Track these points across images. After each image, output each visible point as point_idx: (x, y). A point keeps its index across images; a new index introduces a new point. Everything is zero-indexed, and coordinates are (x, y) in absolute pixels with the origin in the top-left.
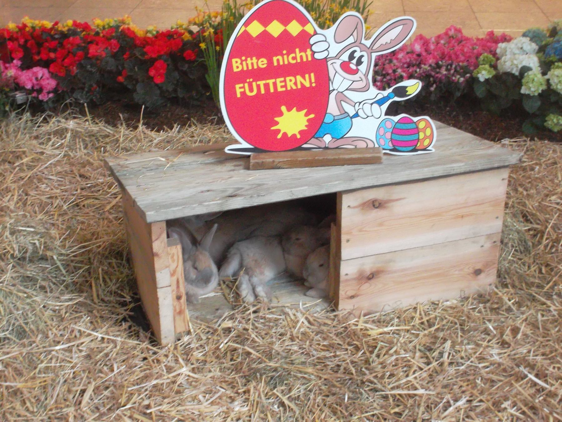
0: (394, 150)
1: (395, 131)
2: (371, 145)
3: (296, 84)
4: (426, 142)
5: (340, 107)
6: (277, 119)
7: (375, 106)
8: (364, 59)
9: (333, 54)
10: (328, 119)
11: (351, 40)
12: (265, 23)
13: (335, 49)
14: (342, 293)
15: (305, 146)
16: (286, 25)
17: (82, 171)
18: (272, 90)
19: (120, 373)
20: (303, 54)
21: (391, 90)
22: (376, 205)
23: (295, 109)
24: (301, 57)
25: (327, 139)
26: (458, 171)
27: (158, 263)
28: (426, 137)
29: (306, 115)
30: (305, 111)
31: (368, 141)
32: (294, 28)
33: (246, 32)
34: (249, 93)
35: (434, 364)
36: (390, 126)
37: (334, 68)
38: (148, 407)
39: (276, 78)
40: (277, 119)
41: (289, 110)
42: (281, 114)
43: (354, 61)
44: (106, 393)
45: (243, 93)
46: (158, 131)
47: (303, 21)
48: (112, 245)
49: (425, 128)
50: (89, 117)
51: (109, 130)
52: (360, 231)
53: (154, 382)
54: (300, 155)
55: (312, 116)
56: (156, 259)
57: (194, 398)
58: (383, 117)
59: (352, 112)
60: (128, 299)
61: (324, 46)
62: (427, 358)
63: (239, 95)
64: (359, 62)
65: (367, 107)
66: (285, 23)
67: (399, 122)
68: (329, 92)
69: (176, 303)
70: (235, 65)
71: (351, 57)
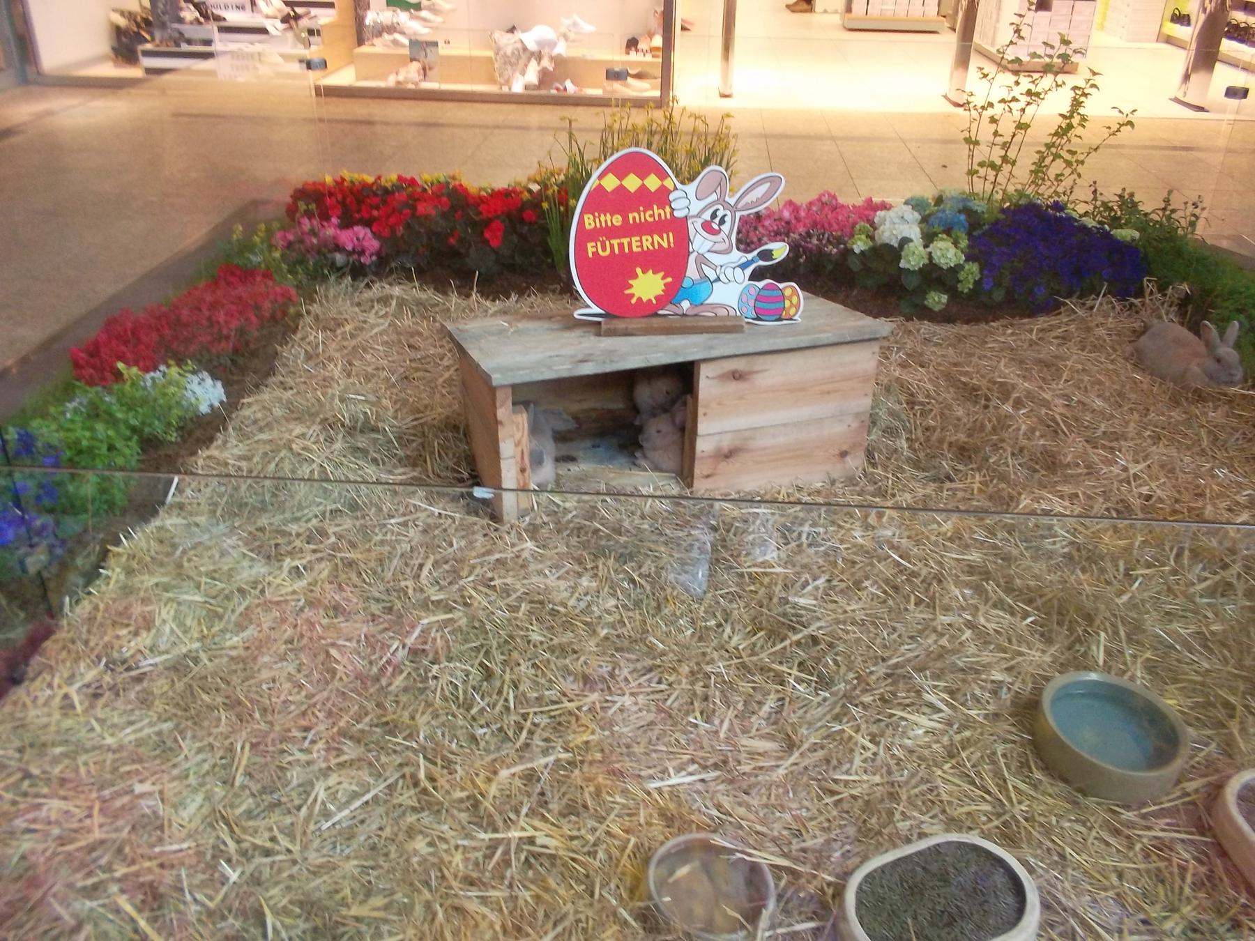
0: (758, 319)
1: (759, 298)
3: (652, 244)
4: (792, 311)
5: (700, 270)
6: (631, 282)
7: (739, 270)
8: (728, 219)
9: (694, 211)
10: (686, 283)
11: (714, 197)
12: (621, 177)
13: (696, 206)
14: (697, 471)
15: (661, 312)
16: (643, 178)
17: (412, 341)
18: (627, 250)
19: (460, 549)
20: (662, 212)
21: (755, 253)
22: (737, 376)
24: (660, 215)
25: (685, 305)
26: (826, 342)
27: (502, 433)
29: (663, 278)
30: (661, 274)
32: (653, 183)
33: (600, 186)
34: (601, 252)
35: (793, 544)
36: (754, 293)
37: (694, 227)
38: (492, 579)
39: (631, 236)
40: (631, 282)
41: (644, 272)
42: (635, 276)
43: (717, 220)
44: (446, 567)
45: (596, 254)
46: (494, 300)
47: (662, 175)
48: (448, 417)
50: (417, 284)
51: (439, 298)
52: (719, 404)
53: (497, 556)
54: (655, 322)
55: (669, 280)
57: (540, 573)
58: (747, 282)
59: (713, 277)
60: (466, 475)
61: (685, 202)
62: (786, 538)
63: (590, 255)
64: (722, 221)
65: (729, 272)
66: (643, 177)
67: (766, 287)
68: (689, 254)
69: (520, 477)
70: (587, 221)
71: (714, 215)
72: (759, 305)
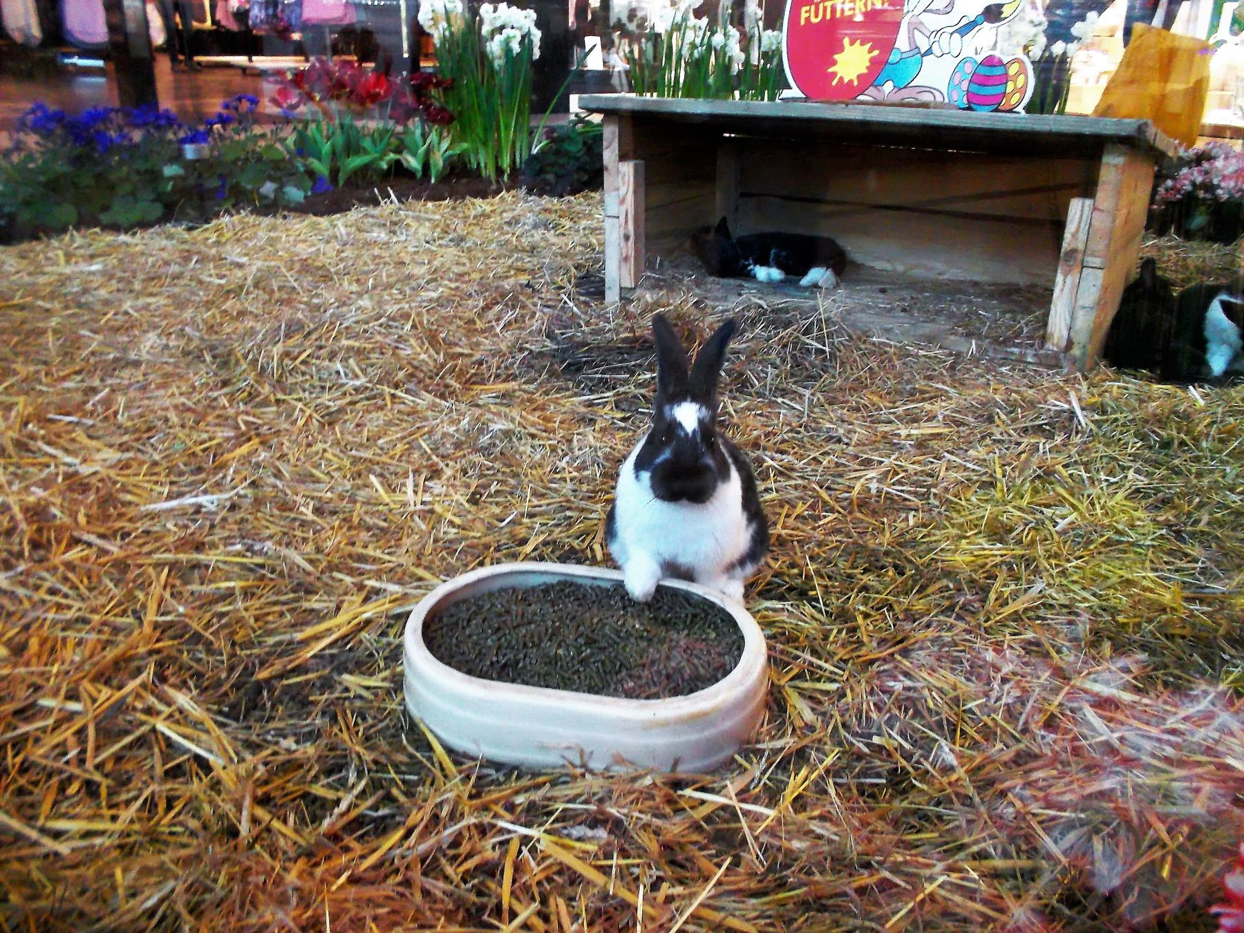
2: (939, 98)
4: (1016, 97)
5: (911, 39)
7: (957, 36)
10: (893, 58)
15: (861, 98)
23: (858, 42)
25: (888, 87)
28: (1014, 92)
29: (870, 51)
30: (869, 45)
31: (937, 94)
40: (836, 57)
45: (808, 19)
49: (1018, 74)
55: (876, 52)
56: (606, 174)
63: (803, 22)
69: (623, 244)
72: (974, 88)
